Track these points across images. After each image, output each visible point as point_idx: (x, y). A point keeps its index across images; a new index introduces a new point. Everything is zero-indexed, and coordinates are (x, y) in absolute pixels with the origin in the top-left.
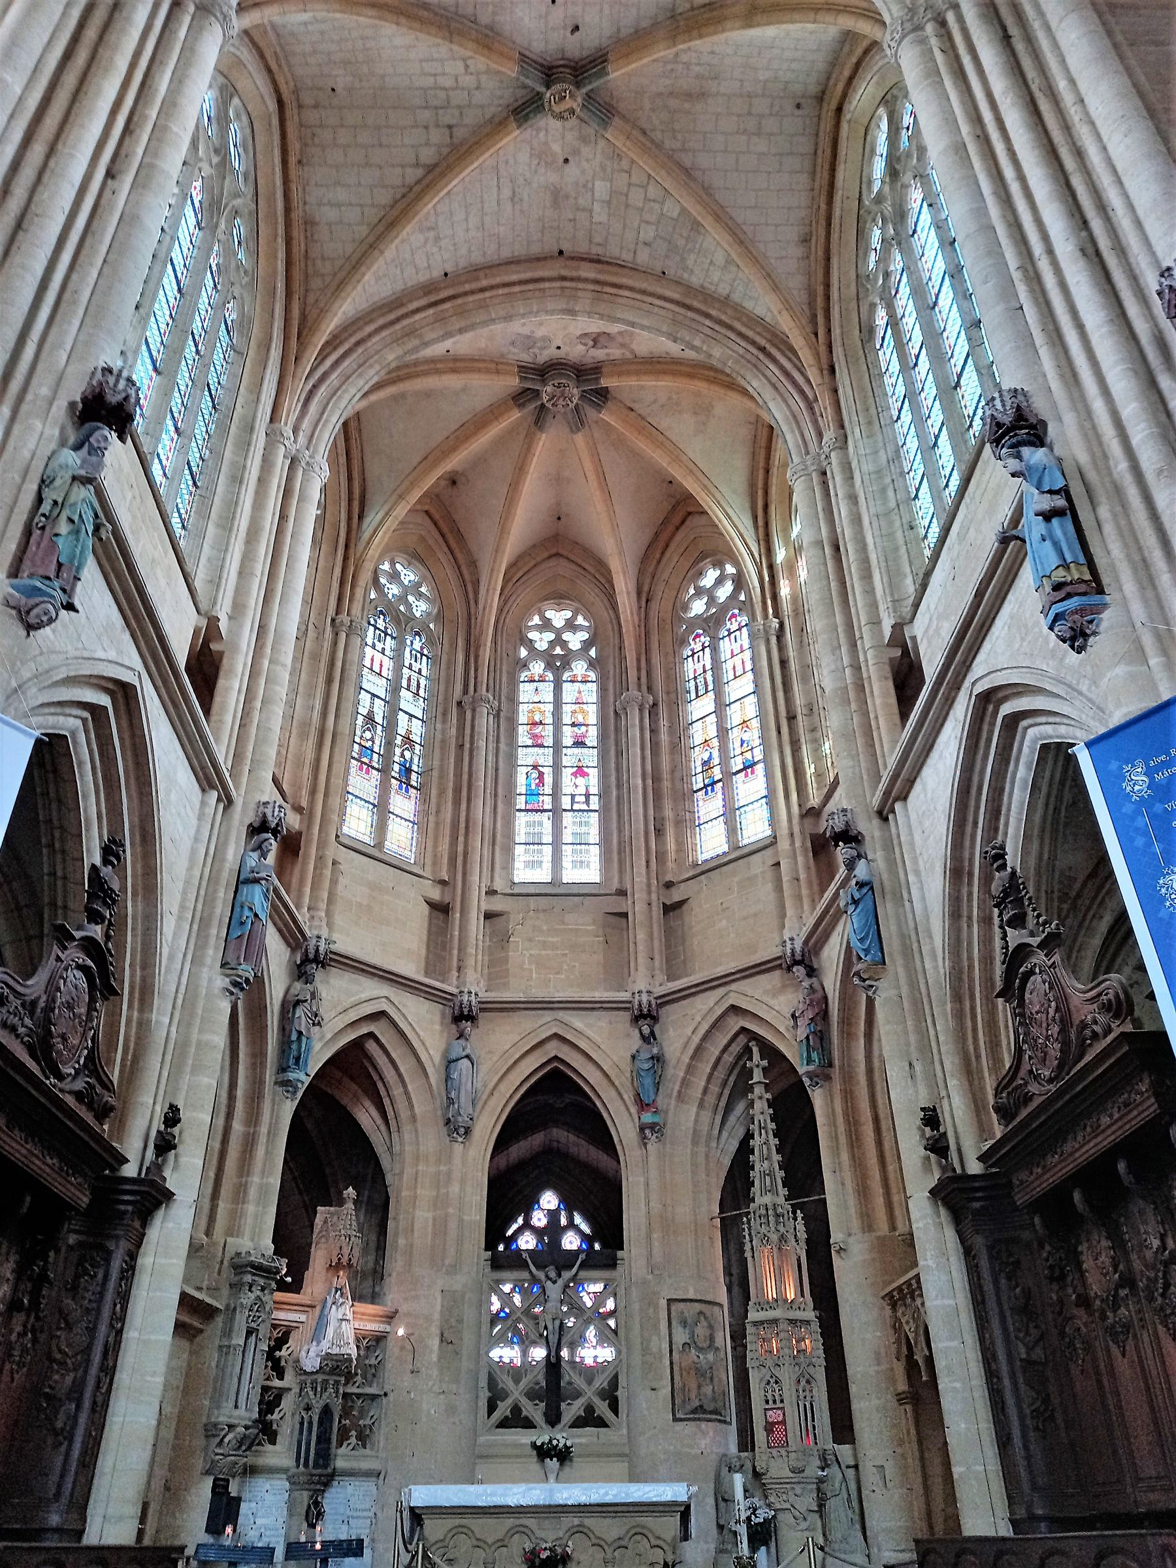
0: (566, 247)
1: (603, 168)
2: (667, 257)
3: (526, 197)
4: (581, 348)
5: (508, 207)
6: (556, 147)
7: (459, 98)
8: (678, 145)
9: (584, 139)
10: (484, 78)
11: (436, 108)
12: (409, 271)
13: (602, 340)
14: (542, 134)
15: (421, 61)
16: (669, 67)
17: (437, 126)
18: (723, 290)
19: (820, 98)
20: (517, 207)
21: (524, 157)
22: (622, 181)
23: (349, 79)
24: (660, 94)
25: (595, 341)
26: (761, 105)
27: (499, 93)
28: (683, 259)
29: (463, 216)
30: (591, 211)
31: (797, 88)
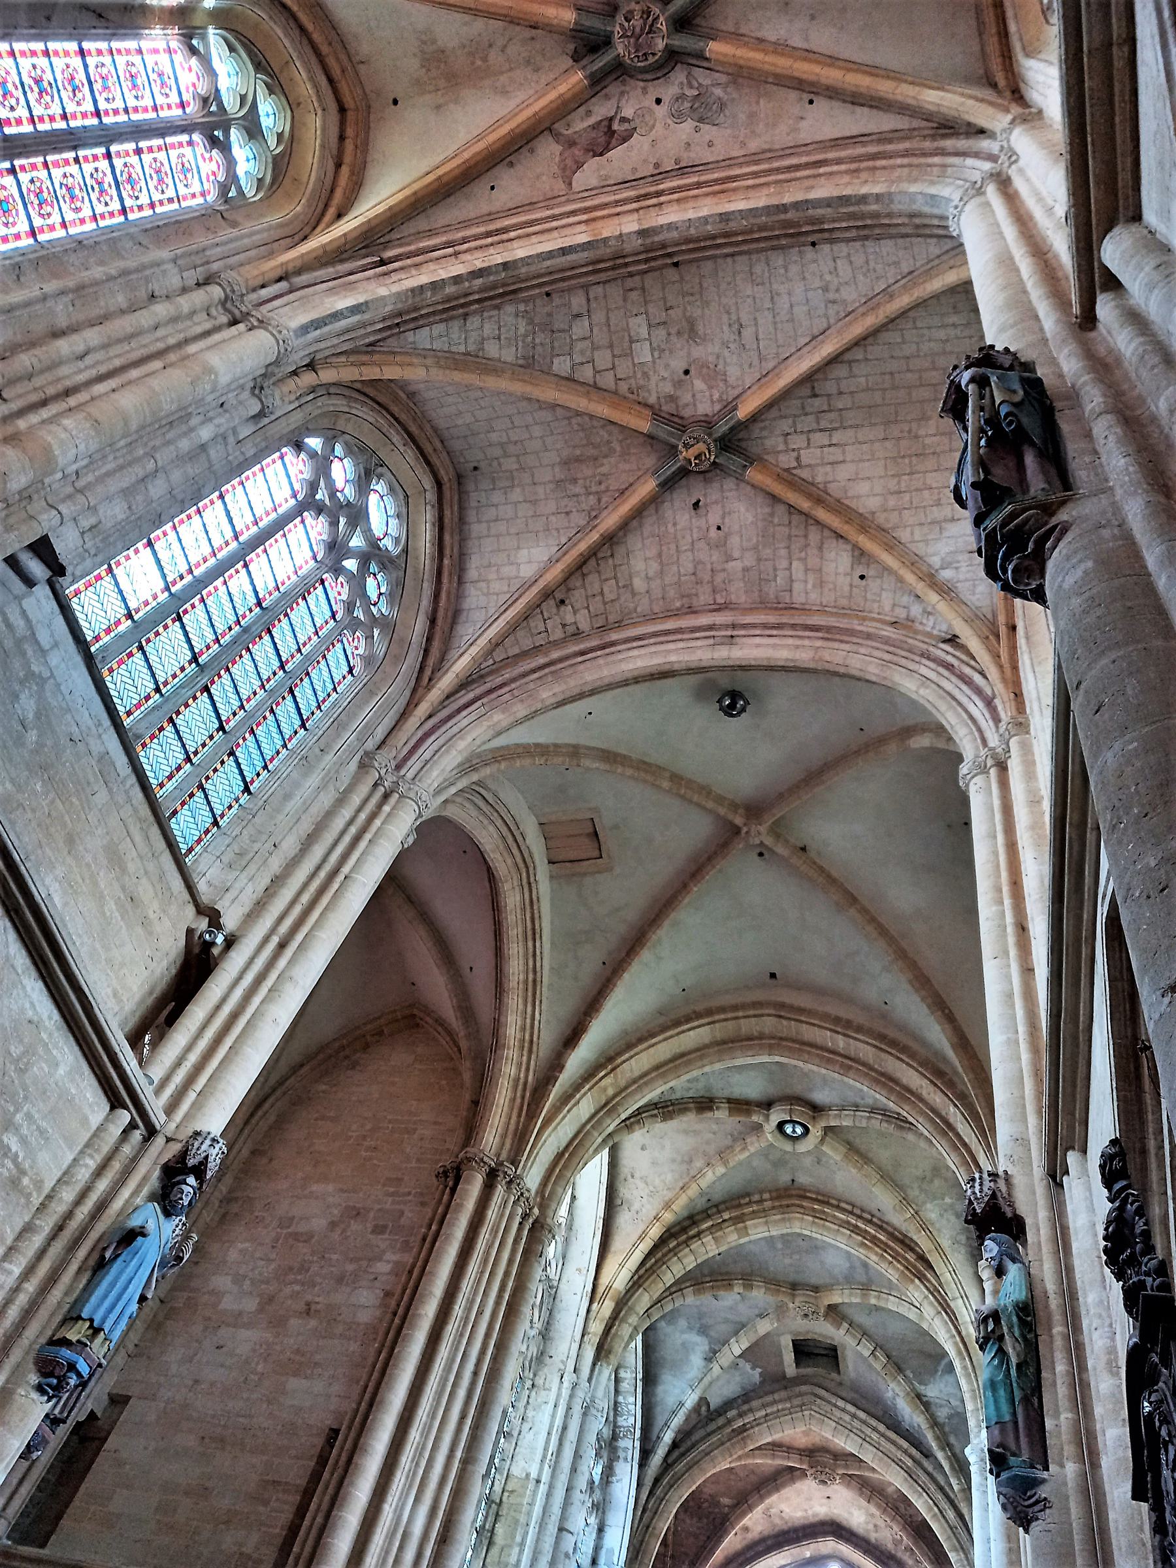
0: (672, 274)
1: (646, 375)
2: (550, 315)
3: (725, 328)
4: (628, 112)
5: (745, 318)
6: (699, 384)
7: (808, 422)
8: (574, 421)
9: (672, 398)
10: (781, 447)
11: (830, 411)
12: (859, 259)
13: (602, 140)
14: (716, 396)
15: (844, 462)
16: (603, 487)
17: (829, 395)
18: (474, 322)
19: (460, 478)
20: (734, 317)
21: (733, 372)
22: (623, 368)
23: (922, 432)
24: (606, 456)
25: (610, 133)
26: (510, 464)
27: (765, 433)
28: (531, 322)
29: (796, 310)
30: (650, 326)
31: (485, 484)
